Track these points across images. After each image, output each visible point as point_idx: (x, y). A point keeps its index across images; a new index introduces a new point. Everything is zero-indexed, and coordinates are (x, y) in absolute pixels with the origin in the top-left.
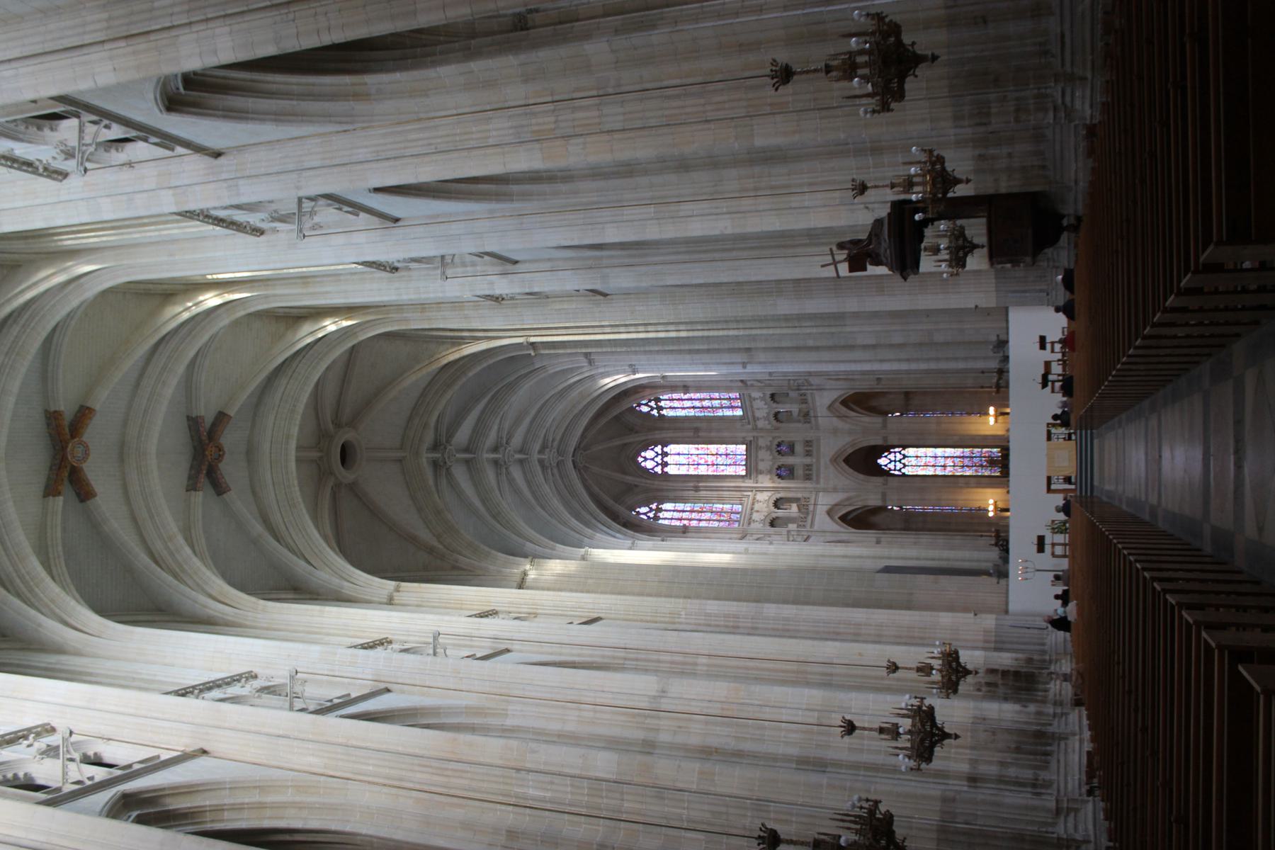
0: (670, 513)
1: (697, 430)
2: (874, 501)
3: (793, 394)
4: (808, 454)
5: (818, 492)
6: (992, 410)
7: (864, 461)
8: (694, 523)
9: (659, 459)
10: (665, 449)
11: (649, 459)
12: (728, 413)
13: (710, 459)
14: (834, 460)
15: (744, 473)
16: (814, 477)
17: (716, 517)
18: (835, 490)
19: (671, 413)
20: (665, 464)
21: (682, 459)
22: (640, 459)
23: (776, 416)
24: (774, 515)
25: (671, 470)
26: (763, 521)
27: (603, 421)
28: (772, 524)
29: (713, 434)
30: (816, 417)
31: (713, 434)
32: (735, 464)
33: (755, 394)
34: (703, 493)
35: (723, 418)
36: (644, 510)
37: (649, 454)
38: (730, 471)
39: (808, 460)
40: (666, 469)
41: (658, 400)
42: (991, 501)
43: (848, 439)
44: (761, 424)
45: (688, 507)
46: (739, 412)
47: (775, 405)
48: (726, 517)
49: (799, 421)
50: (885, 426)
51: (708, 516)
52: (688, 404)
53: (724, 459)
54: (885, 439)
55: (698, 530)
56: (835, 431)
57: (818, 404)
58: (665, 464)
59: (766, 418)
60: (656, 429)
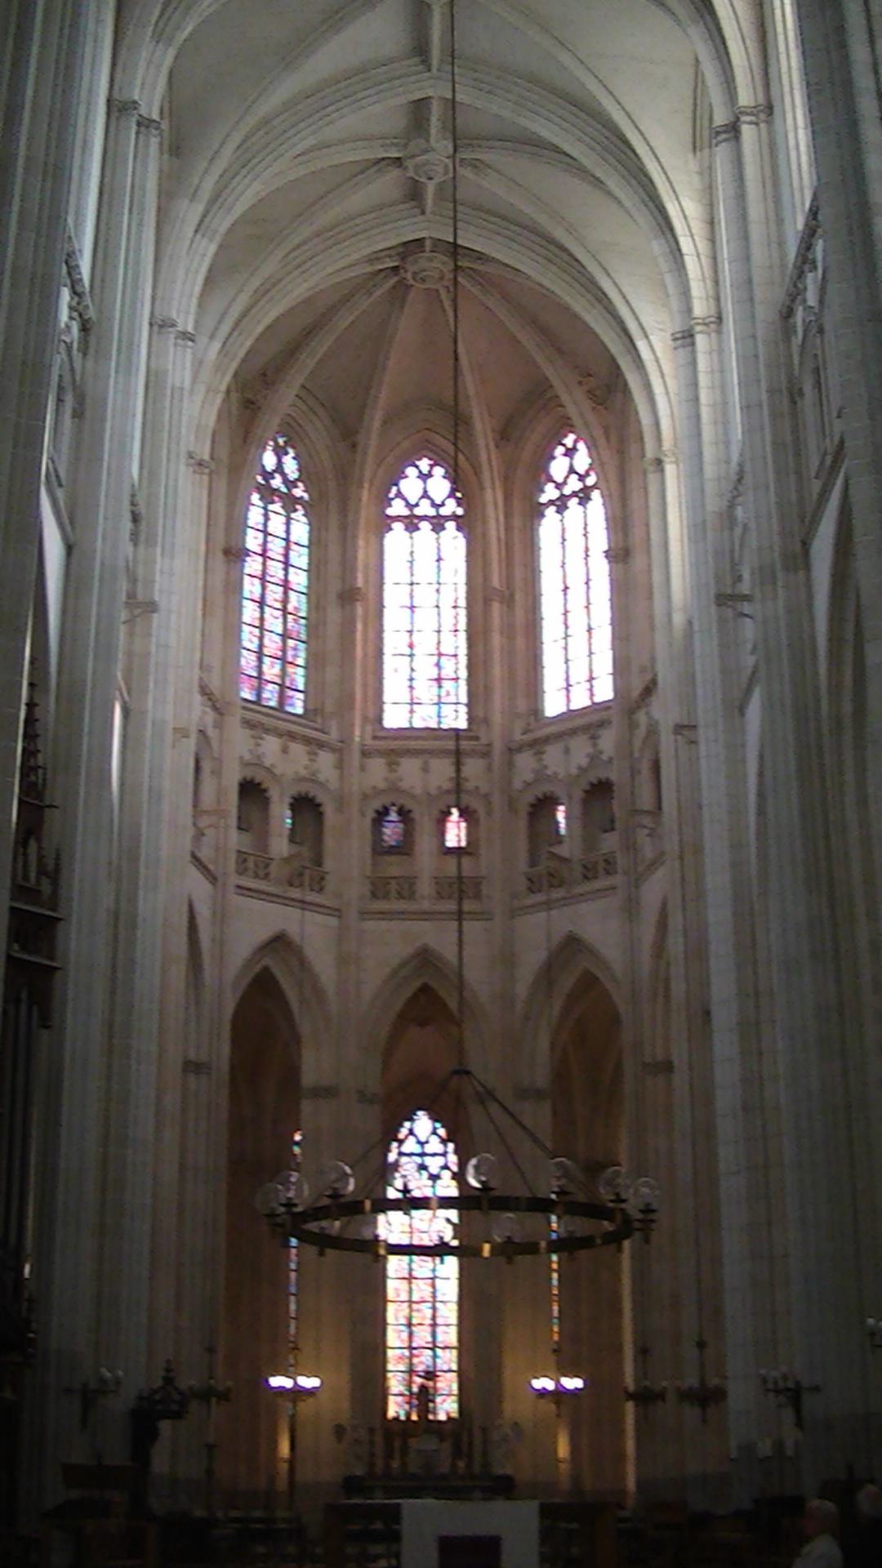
2: (314, 1066)
3: (610, 842)
5: (336, 912)
6: (573, 1383)
8: (251, 588)
9: (425, 509)
10: (451, 526)
11: (425, 485)
14: (425, 958)
17: (272, 644)
18: (344, 961)
21: (425, 570)
22: (424, 464)
23: (544, 806)
24: (274, 793)
25: (396, 540)
27: (528, 339)
28: (252, 792)
30: (548, 905)
31: (497, 640)
33: (608, 741)
34: (334, 614)
36: (291, 466)
37: (439, 486)
39: (425, 887)
40: (398, 527)
41: (584, 496)
42: (309, 1382)
44: (525, 762)
45: (299, 579)
46: (553, 705)
47: (578, 794)
48: (271, 670)
49: (533, 862)
50: (523, 1093)
51: (274, 623)
56: (507, 959)
57: (584, 907)
58: (411, 523)
59: (540, 776)
60: (507, 498)
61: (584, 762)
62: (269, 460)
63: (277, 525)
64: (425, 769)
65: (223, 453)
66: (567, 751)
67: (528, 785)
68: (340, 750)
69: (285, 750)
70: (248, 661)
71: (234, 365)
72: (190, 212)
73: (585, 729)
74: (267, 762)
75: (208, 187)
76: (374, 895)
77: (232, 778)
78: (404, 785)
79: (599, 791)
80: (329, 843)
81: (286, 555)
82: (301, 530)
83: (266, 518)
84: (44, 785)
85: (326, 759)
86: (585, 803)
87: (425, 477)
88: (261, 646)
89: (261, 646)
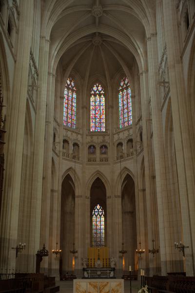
0: (70, 96)
1: (112, 107)
2: (78, 192)
4: (101, 160)
7: (98, 194)
9: (97, 92)
10: (102, 96)
12: (121, 122)
13: (98, 115)
14: (98, 172)
15: (91, 131)
16: (89, 163)
19: (120, 96)
20: (95, 95)
23: (120, 144)
24: (70, 142)
25: (92, 99)
26: (67, 136)
28: (65, 141)
29: (110, 114)
32: (96, 127)
34: (81, 111)
35: (118, 119)
36: (73, 84)
37: (100, 89)
38: (92, 124)
39: (98, 159)
40: (93, 96)
41: (127, 88)
43: (109, 179)
44: (116, 137)
45: (75, 105)
48: (69, 121)
50: (116, 197)
52: (125, 102)
53: (98, 120)
54: (110, 197)
55: (62, 104)
57: (127, 162)
58: (95, 95)
61: (127, 136)
62: (69, 82)
63: (70, 94)
64: (98, 138)
65: (59, 79)
66: (124, 134)
67: (116, 141)
68: (82, 135)
69: (72, 134)
70: (64, 118)
71: (60, 57)
72: (47, 14)
73: (127, 130)
74: (69, 136)
75: (52, 8)
76: (89, 161)
77: (62, 139)
78: (94, 141)
79: (130, 141)
80: (80, 152)
81: (72, 100)
82: (75, 96)
83: (68, 92)
84: (2, 101)
85: (79, 136)
86: (127, 143)
87: (97, 87)
88: (67, 116)
89: (67, 116)
